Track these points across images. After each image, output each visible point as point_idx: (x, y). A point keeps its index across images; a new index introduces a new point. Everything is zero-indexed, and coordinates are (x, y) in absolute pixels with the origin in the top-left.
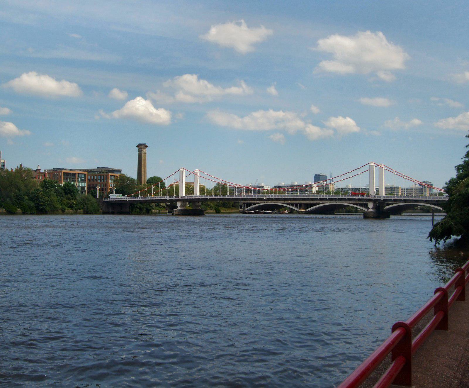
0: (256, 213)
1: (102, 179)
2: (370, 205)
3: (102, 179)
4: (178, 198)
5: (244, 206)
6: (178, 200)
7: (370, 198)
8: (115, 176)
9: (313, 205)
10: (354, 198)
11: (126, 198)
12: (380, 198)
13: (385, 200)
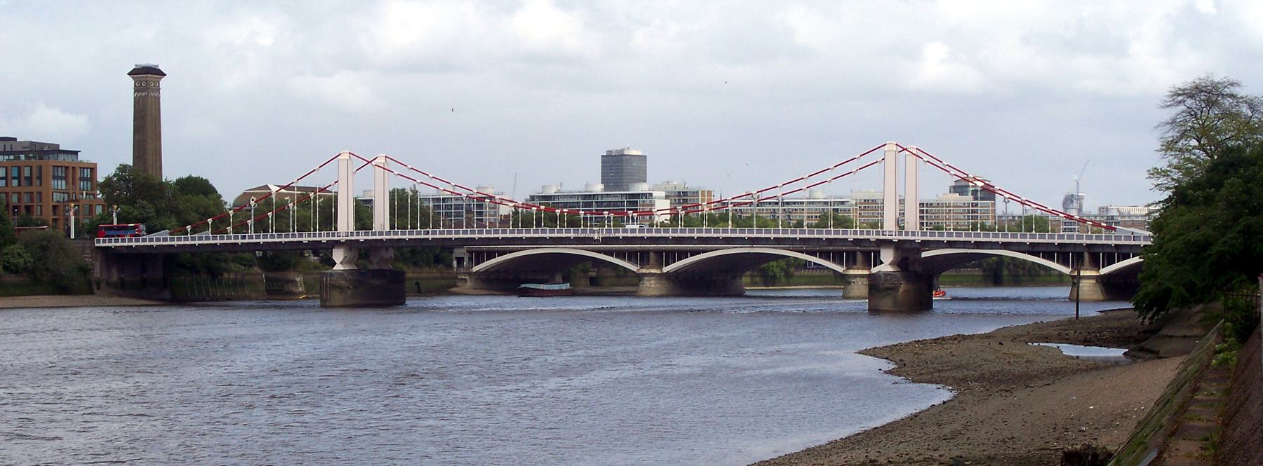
2: (887, 256)
3: (14, 178)
4: (336, 238)
5: (471, 259)
7: (887, 237)
8: (67, 168)
9: (683, 254)
10: (845, 237)
11: (165, 240)
12: (913, 238)
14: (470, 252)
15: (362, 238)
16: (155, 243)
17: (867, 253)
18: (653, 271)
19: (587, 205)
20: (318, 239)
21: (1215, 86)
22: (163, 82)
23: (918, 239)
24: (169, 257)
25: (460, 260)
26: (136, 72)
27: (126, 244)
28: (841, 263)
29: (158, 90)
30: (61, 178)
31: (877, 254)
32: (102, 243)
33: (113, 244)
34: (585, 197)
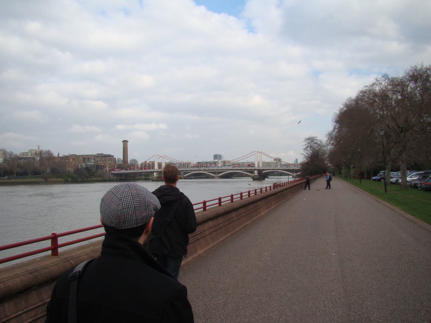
0: (191, 179)
1: (103, 161)
2: (256, 172)
4: (154, 171)
5: (184, 174)
6: (155, 172)
8: (111, 159)
9: (222, 172)
10: (248, 168)
12: (260, 168)
13: (263, 169)
14: (184, 173)
15: (159, 170)
16: (122, 172)
17: (252, 172)
18: (216, 175)
19: (206, 164)
20: (151, 171)
21: (313, 138)
22: (128, 143)
23: (262, 169)
24: (126, 174)
25: (182, 174)
26: (124, 141)
27: (128, 172)
28: (250, 173)
29: (127, 144)
30: (110, 161)
31: (254, 171)
32: (113, 172)
33: (115, 172)
34: (206, 162)
